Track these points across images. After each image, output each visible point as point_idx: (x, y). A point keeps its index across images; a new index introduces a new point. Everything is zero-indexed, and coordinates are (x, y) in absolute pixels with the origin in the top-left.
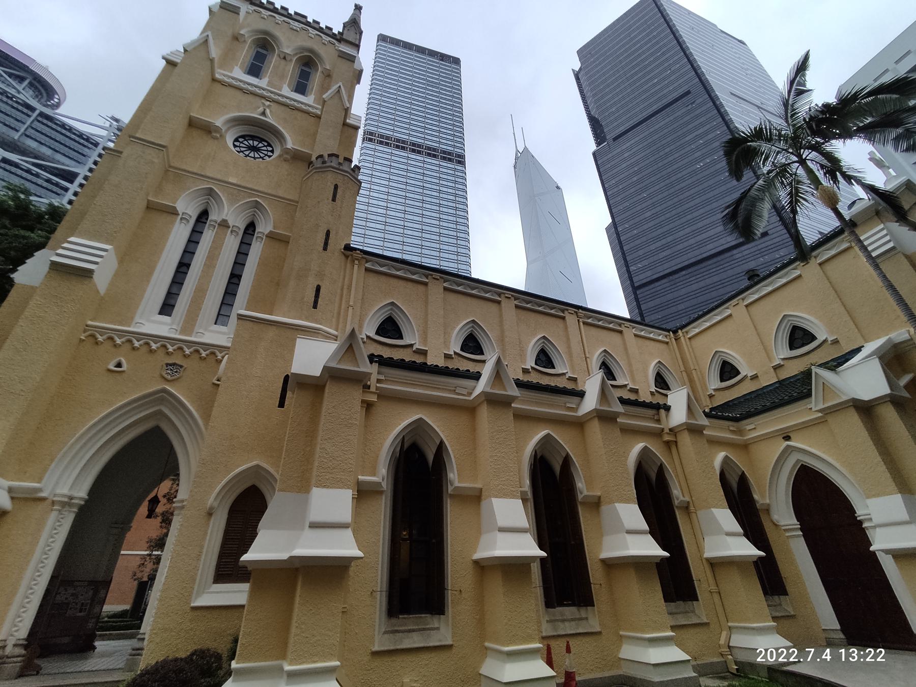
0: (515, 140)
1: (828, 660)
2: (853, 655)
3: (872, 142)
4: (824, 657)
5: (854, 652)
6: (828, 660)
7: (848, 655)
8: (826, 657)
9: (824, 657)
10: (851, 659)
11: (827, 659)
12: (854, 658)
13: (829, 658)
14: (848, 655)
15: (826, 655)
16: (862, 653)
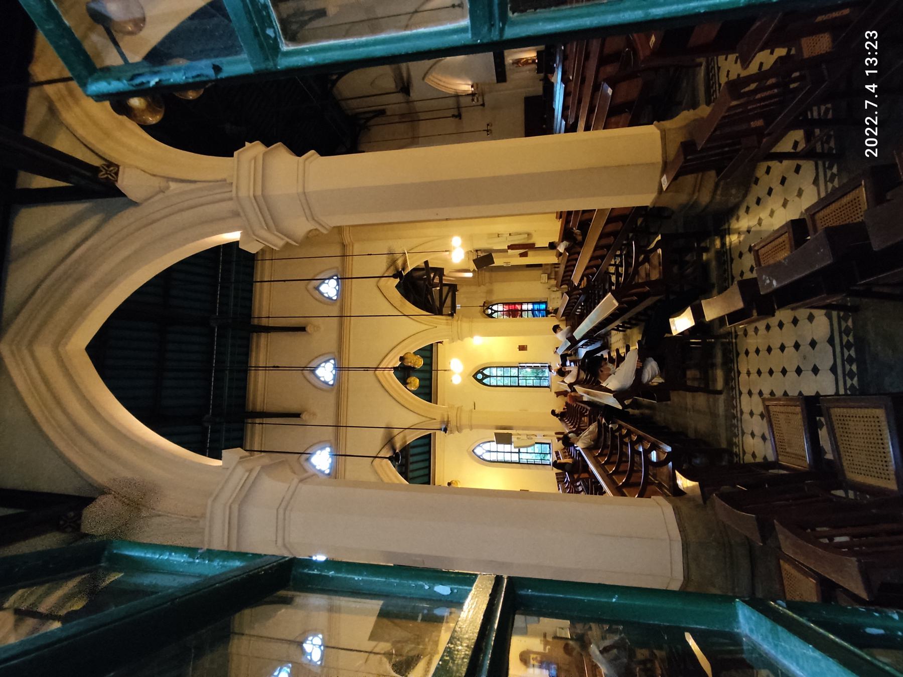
0: (284, 281)
1: (876, 86)
2: (871, 62)
3: (69, 99)
4: (873, 91)
5: (868, 62)
6: (876, 86)
7: (871, 67)
8: (874, 89)
9: (873, 91)
10: (875, 64)
11: (875, 88)
12: (874, 62)
13: (874, 86)
14: (871, 67)
15: (872, 88)
16: (869, 53)
